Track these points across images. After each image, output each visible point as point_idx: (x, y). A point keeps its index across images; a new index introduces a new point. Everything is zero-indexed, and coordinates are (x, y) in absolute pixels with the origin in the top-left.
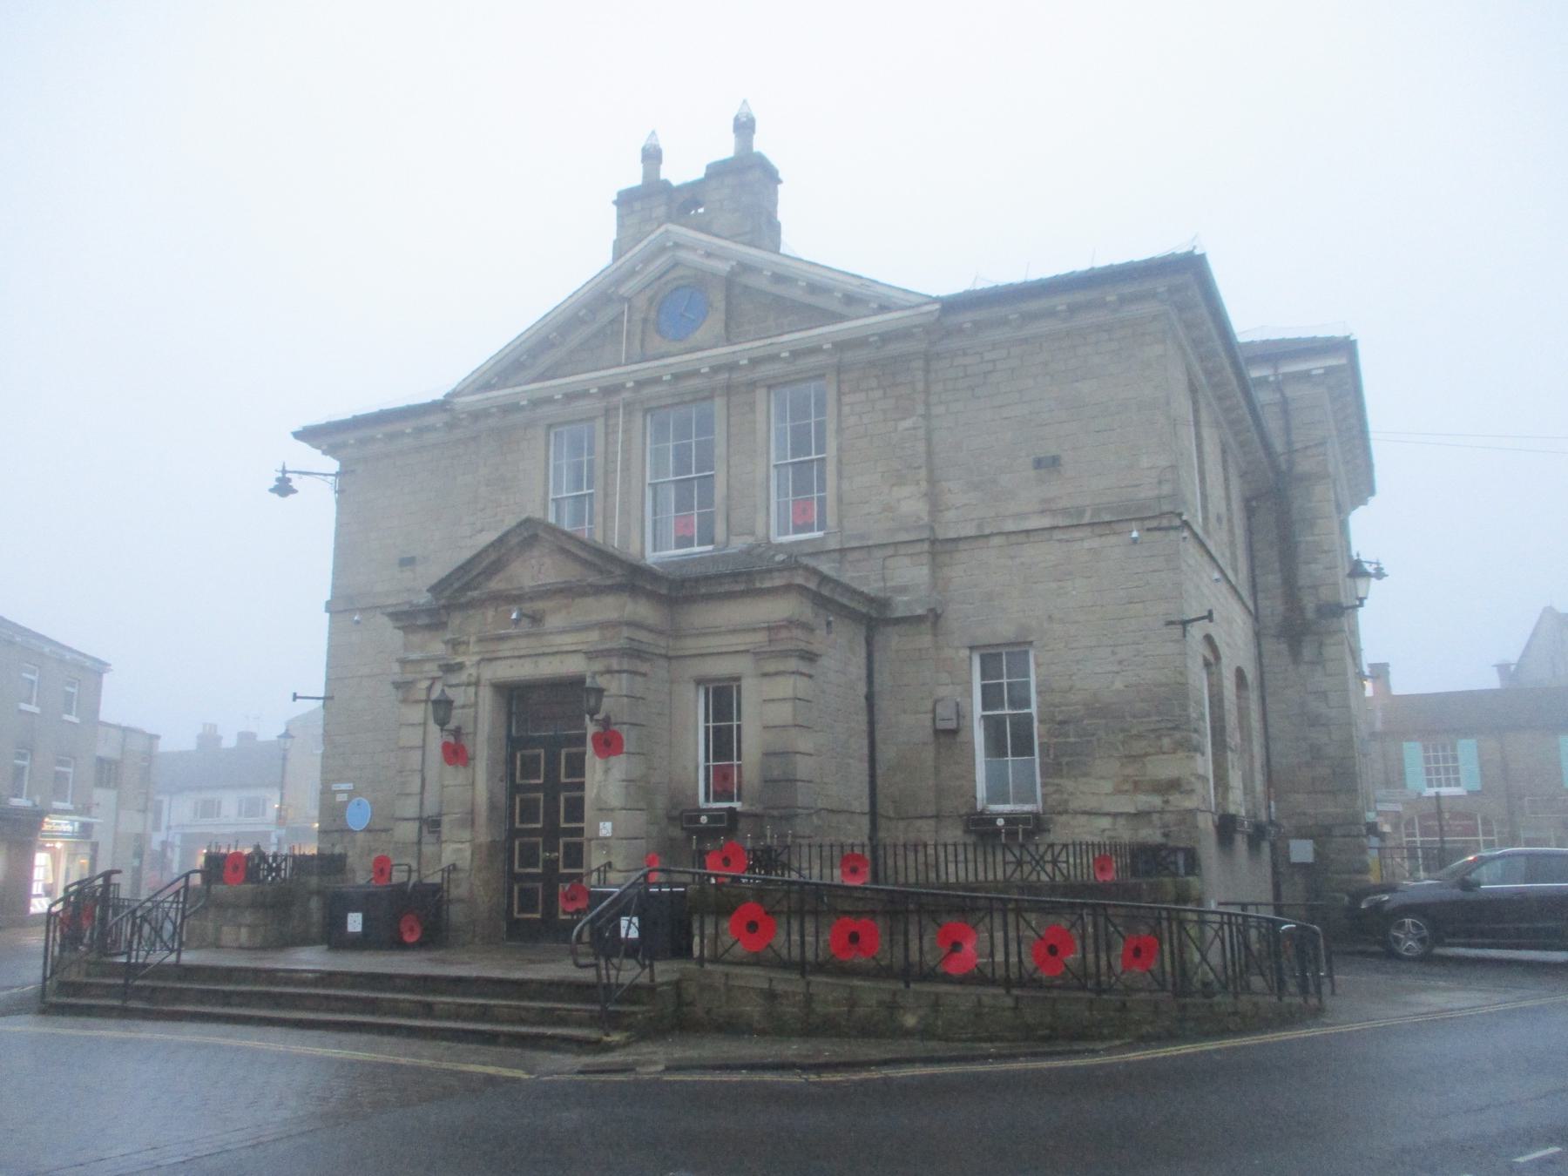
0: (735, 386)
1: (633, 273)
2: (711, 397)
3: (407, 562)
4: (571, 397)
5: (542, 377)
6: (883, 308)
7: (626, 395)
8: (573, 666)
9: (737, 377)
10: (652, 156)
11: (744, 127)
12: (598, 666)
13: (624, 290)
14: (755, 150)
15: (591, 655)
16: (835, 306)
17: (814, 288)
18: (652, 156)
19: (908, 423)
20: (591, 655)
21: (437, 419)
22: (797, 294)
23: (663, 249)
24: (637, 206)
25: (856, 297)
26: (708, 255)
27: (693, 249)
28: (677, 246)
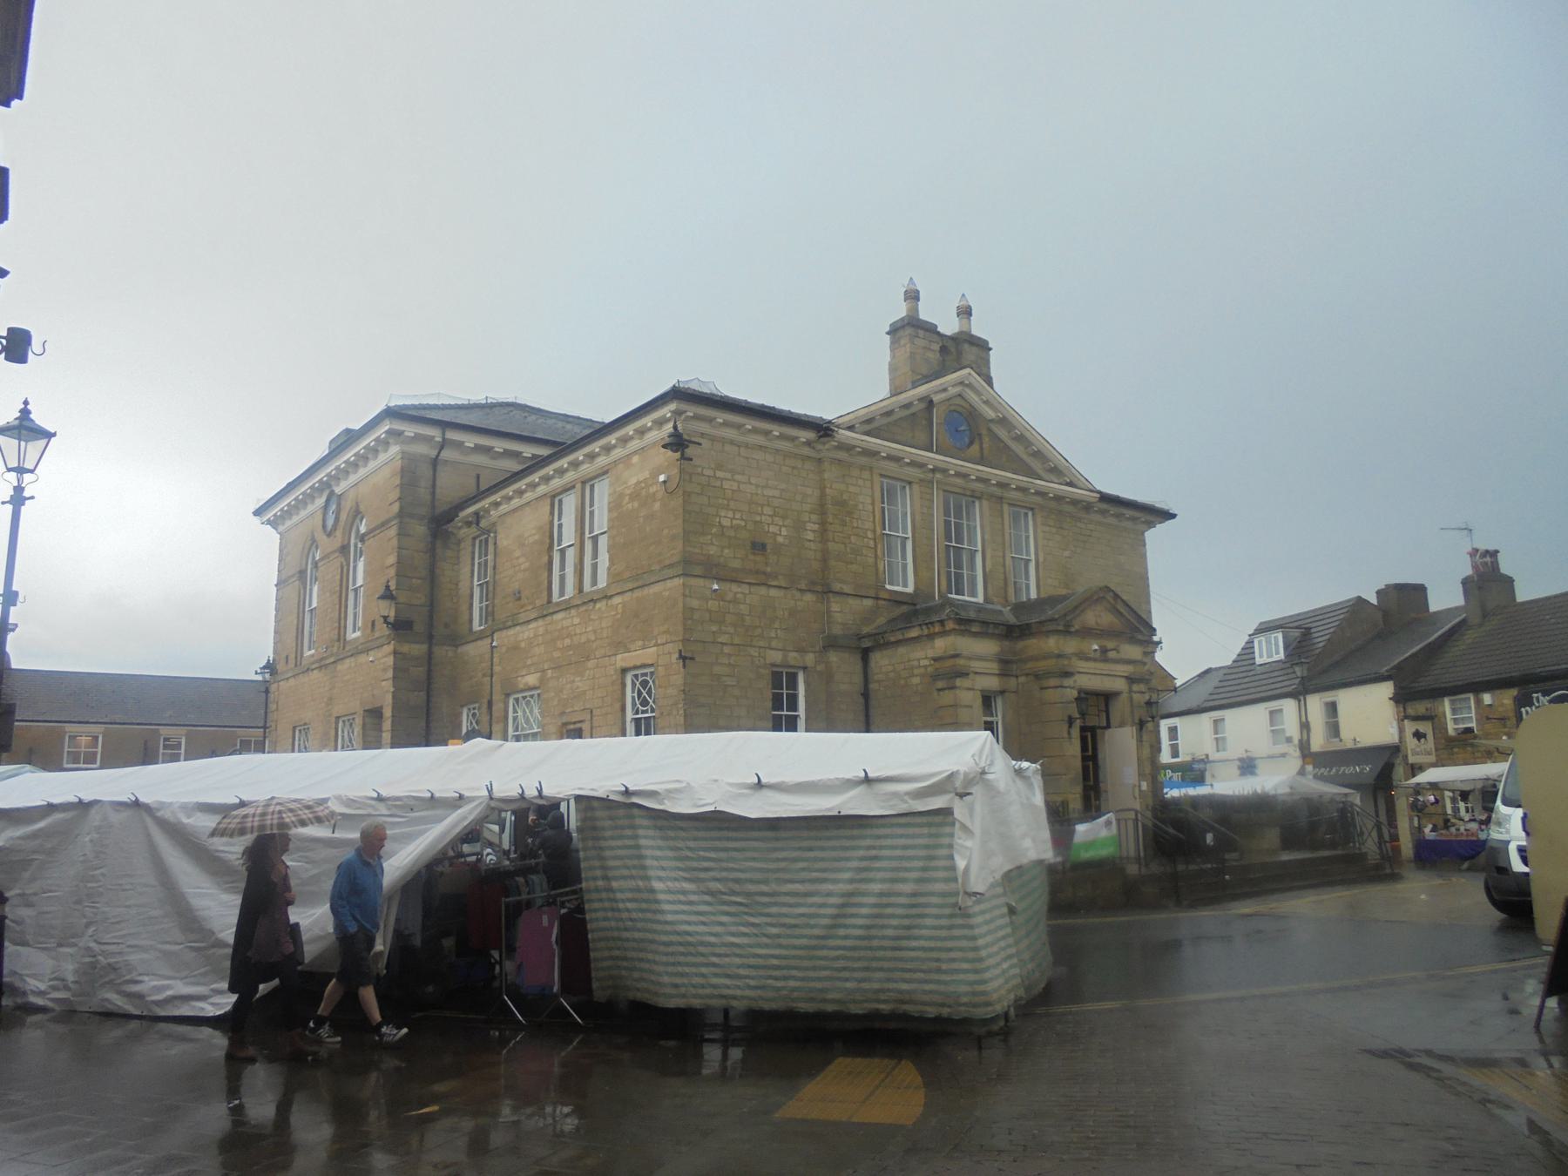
0: (998, 496)
1: (945, 390)
2: (979, 498)
3: (759, 547)
4: (913, 464)
5: (868, 433)
6: (1070, 484)
7: (938, 476)
8: (1119, 685)
9: (998, 491)
10: (913, 296)
11: (965, 312)
12: (1135, 687)
13: (936, 398)
14: (974, 332)
15: (1131, 680)
16: (1036, 465)
17: (1038, 455)
18: (913, 296)
19: (1067, 553)
20: (1131, 680)
21: (805, 435)
22: (1018, 448)
23: (962, 383)
24: (921, 333)
25: (1058, 470)
26: (986, 402)
27: (978, 393)
28: (970, 386)
